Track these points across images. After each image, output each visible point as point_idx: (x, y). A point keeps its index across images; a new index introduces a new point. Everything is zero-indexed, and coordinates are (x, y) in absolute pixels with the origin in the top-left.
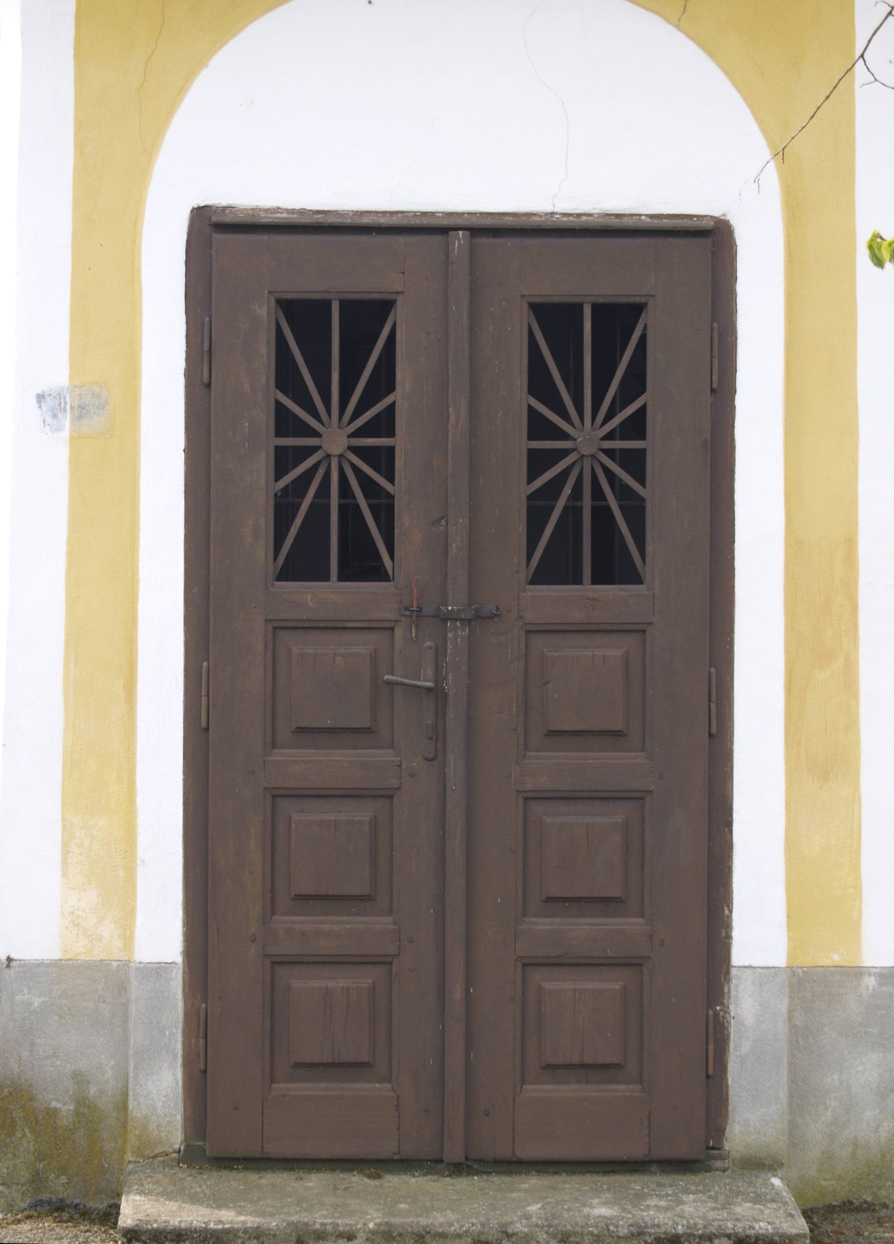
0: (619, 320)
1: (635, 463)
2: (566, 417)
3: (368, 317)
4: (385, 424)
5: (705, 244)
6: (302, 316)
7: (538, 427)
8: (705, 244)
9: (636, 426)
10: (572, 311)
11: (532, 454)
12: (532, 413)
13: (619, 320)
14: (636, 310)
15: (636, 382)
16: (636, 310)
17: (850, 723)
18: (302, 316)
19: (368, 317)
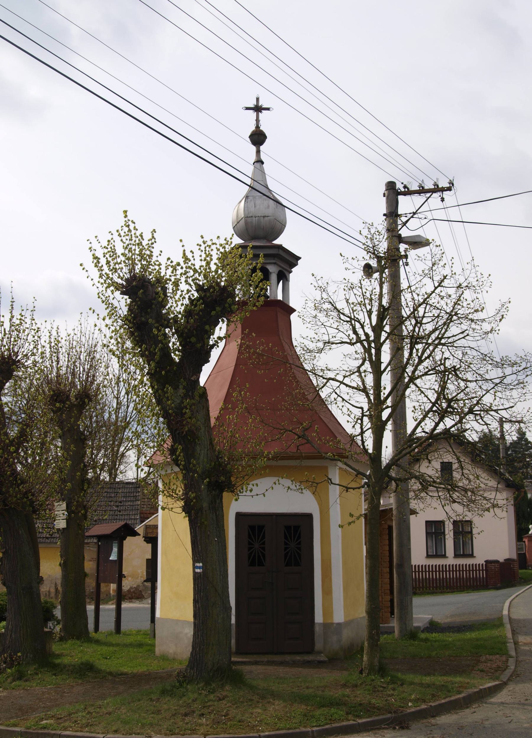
0: (297, 528)
1: (299, 549)
2: (253, 541)
3: (261, 528)
4: (264, 543)
5: (309, 517)
6: (252, 528)
7: (286, 544)
8: (309, 517)
9: (299, 543)
10: (290, 527)
11: (264, 545)
12: (249, 542)
13: (297, 528)
14: (299, 527)
15: (299, 537)
16: (299, 527)
17: (331, 587)
18: (252, 528)
19: (261, 528)
